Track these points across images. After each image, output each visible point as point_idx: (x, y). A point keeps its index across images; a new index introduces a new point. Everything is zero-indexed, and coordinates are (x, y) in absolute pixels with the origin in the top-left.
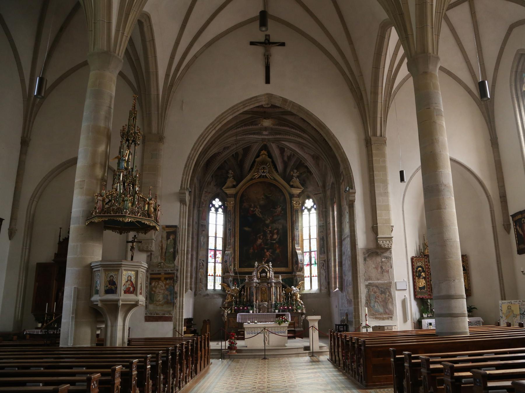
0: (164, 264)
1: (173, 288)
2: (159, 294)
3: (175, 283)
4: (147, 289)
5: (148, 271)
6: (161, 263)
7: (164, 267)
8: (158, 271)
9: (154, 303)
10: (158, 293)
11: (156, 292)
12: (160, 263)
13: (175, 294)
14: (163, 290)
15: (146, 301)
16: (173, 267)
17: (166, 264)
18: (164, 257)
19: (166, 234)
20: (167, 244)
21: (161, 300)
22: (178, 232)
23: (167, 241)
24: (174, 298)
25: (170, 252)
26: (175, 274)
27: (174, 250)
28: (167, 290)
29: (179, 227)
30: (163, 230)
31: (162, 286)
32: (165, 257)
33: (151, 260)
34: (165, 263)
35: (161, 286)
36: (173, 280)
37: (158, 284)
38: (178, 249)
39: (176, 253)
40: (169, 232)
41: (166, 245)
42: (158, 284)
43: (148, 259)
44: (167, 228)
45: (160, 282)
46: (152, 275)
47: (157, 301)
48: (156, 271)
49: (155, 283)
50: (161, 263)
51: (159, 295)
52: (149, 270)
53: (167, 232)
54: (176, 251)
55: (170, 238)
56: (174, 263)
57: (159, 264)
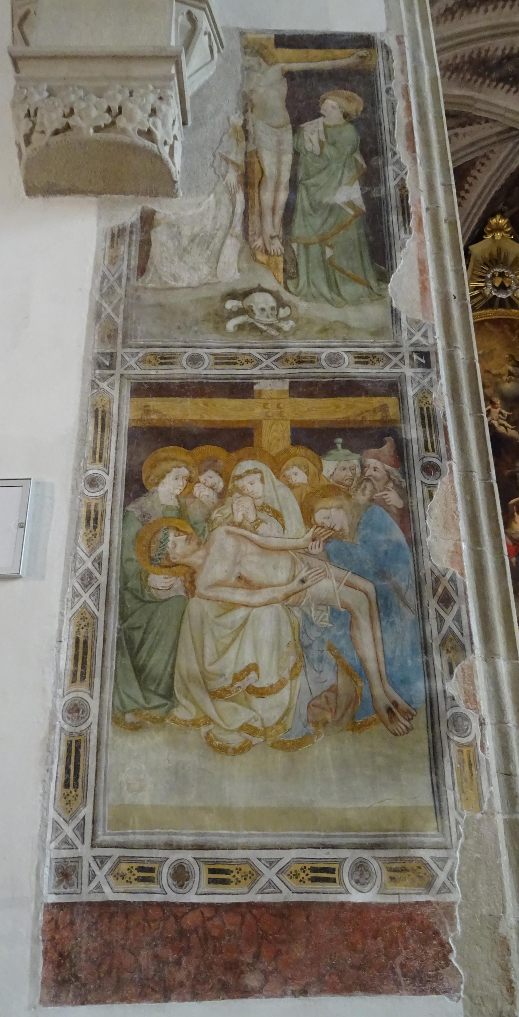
0: (281, 304)
1: (398, 535)
2: (240, 596)
3: (419, 477)
4: (92, 543)
5: (112, 356)
6: (246, 294)
7: (287, 326)
8: (222, 360)
9: (180, 713)
10: (227, 594)
11: (202, 581)
12: (232, 295)
13: (432, 605)
14: (282, 550)
15: (81, 692)
16: (378, 333)
17: (302, 306)
18: (277, 246)
19: (283, 88)
20: (296, 154)
21: (265, 681)
22: (390, 77)
23: (295, 131)
24: (426, 648)
25: (332, 209)
26: (411, 391)
27: (366, 197)
28: (328, 557)
29: (392, 43)
30: (254, 61)
31: (277, 515)
32: (286, 243)
33: (142, 270)
34: (286, 296)
35: (263, 508)
36: (387, 448)
37: (222, 495)
38: (402, 187)
39: (394, 218)
40: (307, 74)
41: (288, 159)
42: (222, 495)
43: (113, 261)
44: (288, 52)
45: (247, 465)
46: (154, 403)
47: (215, 695)
48: (195, 360)
49: (191, 481)
50: (246, 294)
51: (241, 613)
52: (120, 351)
53: (289, 76)
54: (394, 201)
55: (319, 115)
56: (381, 296)
57: (231, 304)
